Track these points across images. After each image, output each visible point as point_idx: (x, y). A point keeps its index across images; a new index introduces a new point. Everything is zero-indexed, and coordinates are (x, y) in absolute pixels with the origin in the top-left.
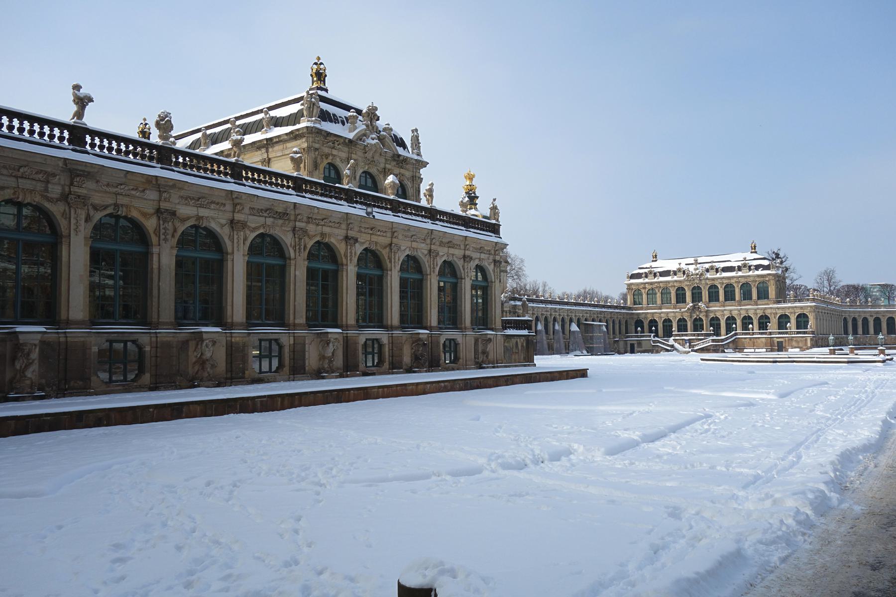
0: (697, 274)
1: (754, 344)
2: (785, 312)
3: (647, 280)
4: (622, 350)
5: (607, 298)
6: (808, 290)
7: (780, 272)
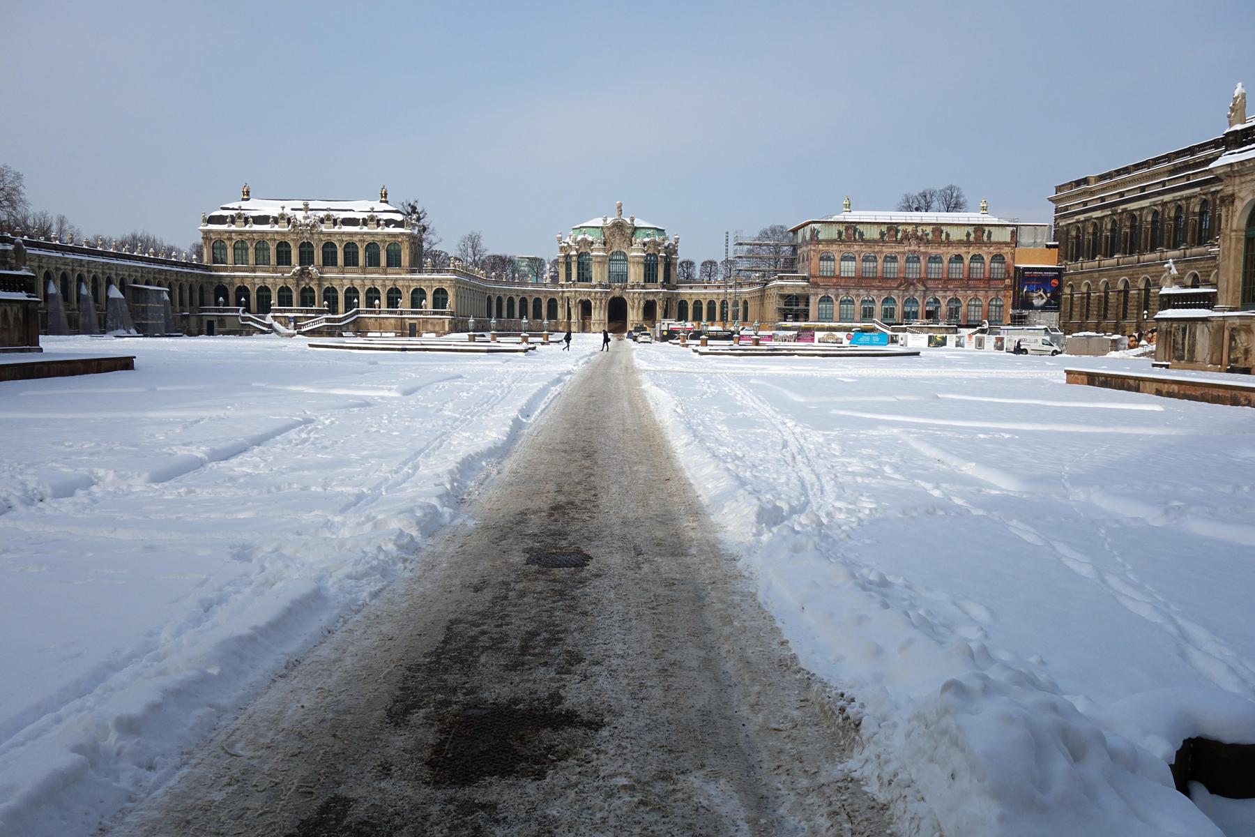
0: (308, 225)
1: (381, 328)
3: (233, 228)
4: (194, 330)
5: (171, 250)
6: (449, 258)
7: (416, 232)
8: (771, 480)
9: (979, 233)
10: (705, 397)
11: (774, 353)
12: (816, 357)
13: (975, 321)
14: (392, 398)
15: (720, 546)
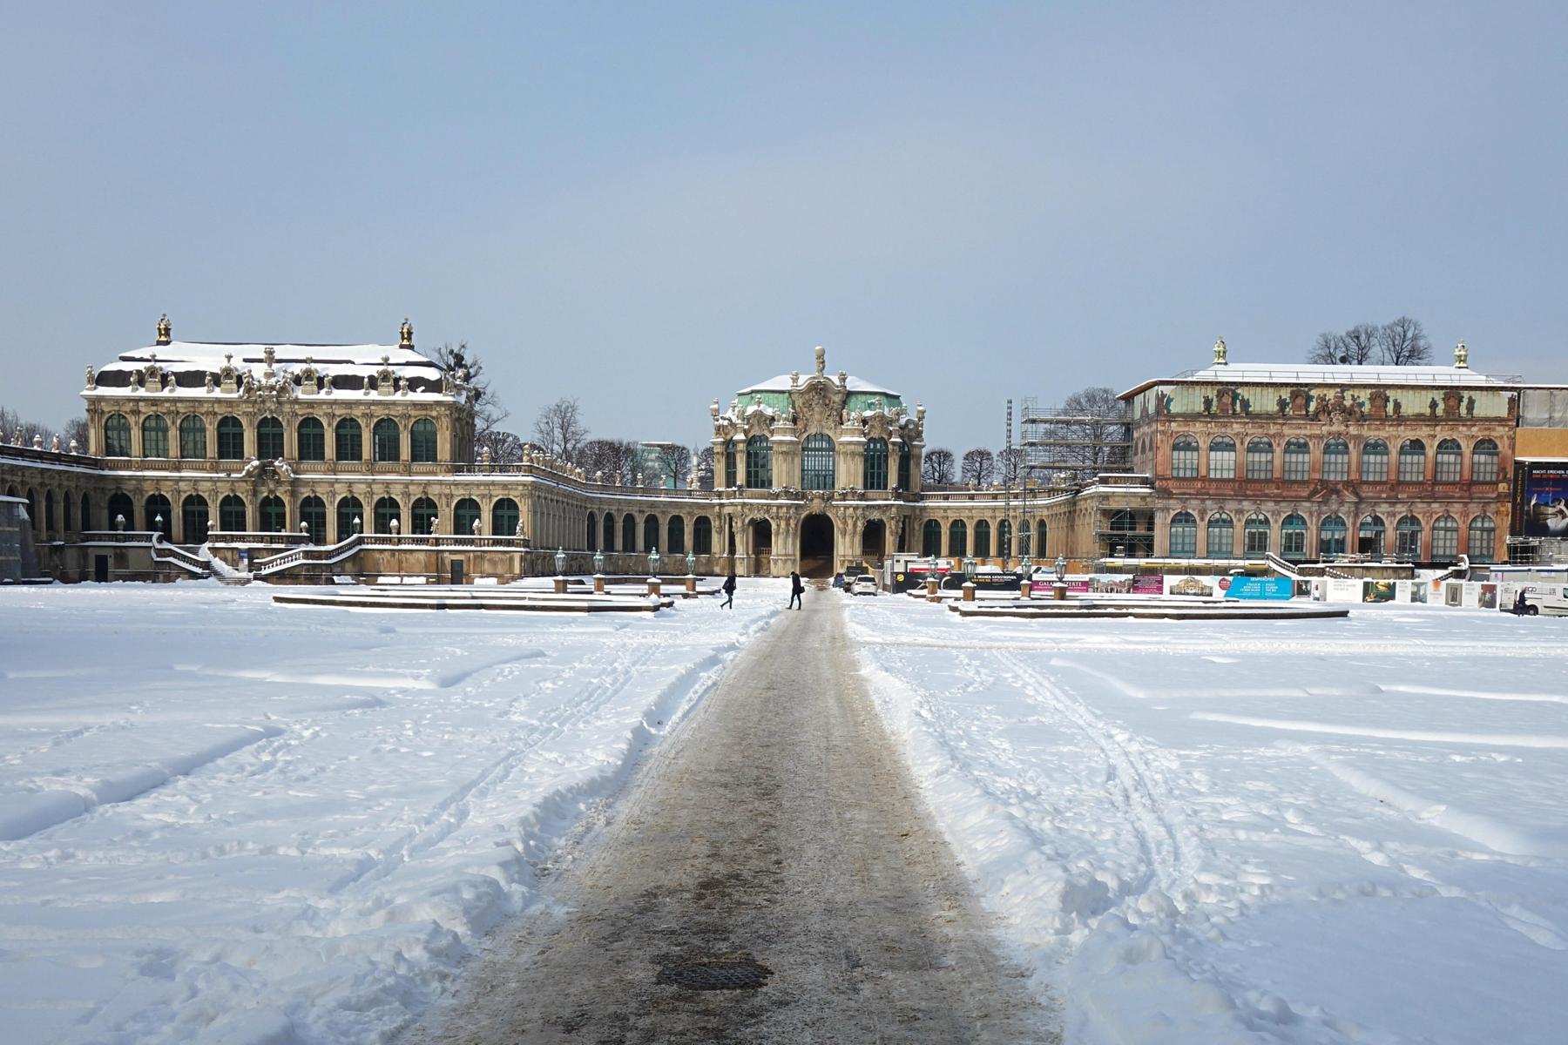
0: (272, 388)
1: (401, 569)
2: (470, 495)
3: (142, 392)
4: (73, 571)
5: (32, 431)
6: (521, 447)
7: (462, 399)
8: (1087, 836)
9: (1452, 402)
10: (970, 689)
11: (1091, 612)
12: (1166, 620)
13: (1445, 556)
14: (421, 692)
15: (997, 952)
